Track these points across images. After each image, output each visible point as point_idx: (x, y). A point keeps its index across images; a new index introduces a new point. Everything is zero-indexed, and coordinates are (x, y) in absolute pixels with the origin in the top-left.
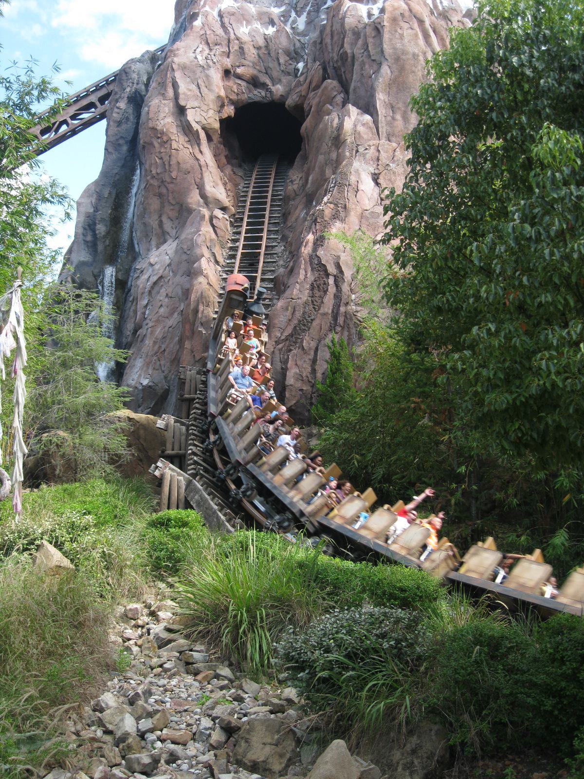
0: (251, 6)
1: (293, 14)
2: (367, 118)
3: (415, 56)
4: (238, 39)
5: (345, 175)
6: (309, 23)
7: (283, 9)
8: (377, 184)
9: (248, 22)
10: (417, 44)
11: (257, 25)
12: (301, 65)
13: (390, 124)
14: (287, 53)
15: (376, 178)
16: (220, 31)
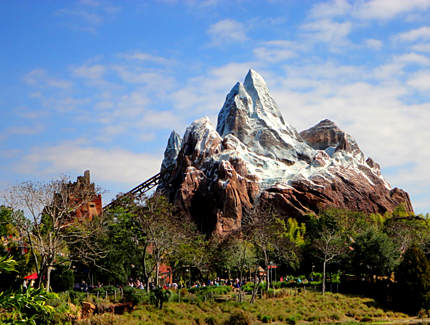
0: (198, 171)
1: (208, 171)
2: (222, 213)
3: (232, 199)
4: (195, 182)
5: (216, 227)
6: (211, 174)
7: (205, 169)
8: (223, 228)
9: (197, 176)
10: (232, 196)
11: (199, 177)
12: (209, 188)
13: (226, 213)
14: (206, 184)
15: (222, 226)
16: (191, 181)
